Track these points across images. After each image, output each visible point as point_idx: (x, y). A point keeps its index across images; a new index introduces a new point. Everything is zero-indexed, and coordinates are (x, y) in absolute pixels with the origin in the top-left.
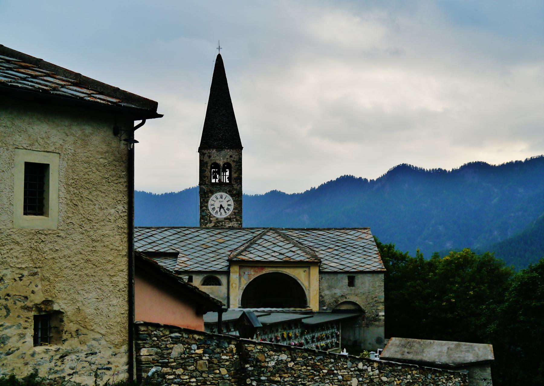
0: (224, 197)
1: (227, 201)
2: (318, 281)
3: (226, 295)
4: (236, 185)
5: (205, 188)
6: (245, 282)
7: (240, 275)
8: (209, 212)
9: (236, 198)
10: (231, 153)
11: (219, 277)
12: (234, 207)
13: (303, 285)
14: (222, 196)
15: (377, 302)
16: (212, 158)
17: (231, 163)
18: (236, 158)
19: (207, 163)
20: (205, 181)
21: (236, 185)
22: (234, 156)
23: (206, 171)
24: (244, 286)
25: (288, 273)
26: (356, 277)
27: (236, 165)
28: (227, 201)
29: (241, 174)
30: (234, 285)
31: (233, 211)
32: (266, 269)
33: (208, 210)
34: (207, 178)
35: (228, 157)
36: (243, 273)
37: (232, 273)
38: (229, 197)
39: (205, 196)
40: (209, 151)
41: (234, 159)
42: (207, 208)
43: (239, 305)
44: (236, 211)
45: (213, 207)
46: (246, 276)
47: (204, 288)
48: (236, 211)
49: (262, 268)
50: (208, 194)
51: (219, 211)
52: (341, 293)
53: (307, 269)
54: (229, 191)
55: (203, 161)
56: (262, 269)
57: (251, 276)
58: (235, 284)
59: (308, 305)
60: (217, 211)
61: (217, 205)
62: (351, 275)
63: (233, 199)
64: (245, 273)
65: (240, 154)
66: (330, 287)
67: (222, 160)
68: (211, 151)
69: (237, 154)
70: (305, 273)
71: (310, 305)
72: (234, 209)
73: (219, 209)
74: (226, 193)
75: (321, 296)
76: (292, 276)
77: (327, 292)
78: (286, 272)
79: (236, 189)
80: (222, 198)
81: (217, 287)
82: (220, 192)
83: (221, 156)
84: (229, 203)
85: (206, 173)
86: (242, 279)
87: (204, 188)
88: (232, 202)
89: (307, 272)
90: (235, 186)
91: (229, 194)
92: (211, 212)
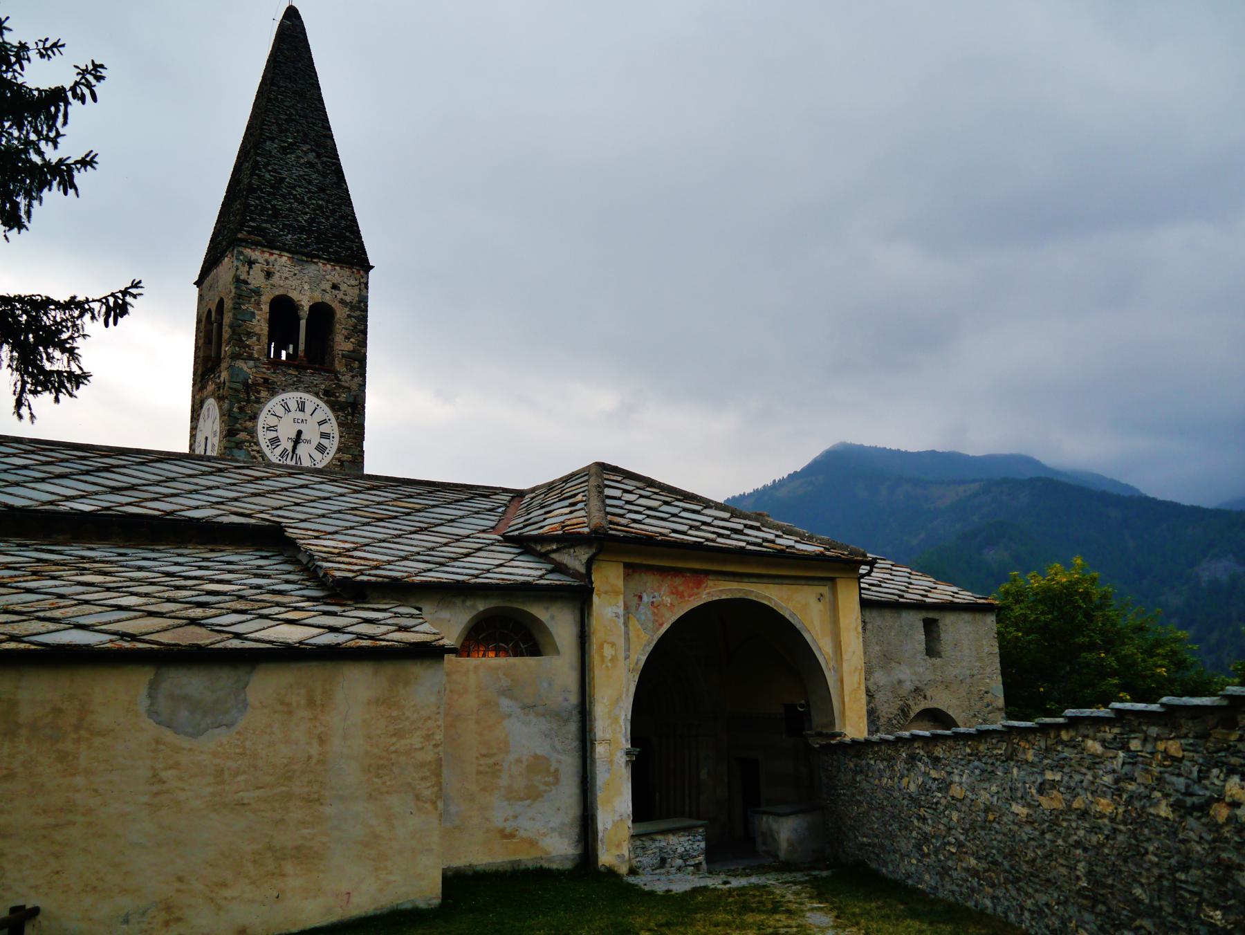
0: (309, 409)
1: (320, 423)
2: (861, 639)
3: (574, 699)
4: (348, 377)
5: (248, 370)
6: (645, 637)
7: (626, 607)
8: (258, 452)
9: (347, 415)
10: (336, 279)
11: (540, 612)
12: (340, 442)
13: (820, 649)
14: (303, 403)
15: (990, 707)
16: (275, 279)
17: (335, 305)
18: (352, 295)
19: (257, 292)
20: (249, 346)
21: (348, 377)
22: (343, 287)
23: (253, 315)
24: (640, 656)
25: (776, 603)
26: (940, 624)
27: (349, 316)
28: (320, 423)
29: (363, 343)
30: (608, 651)
31: (337, 456)
32: (710, 583)
33: (257, 444)
34: (258, 340)
35: (328, 286)
36: (636, 599)
37: (599, 595)
38: (325, 412)
39: (249, 396)
40: (267, 255)
41: (344, 297)
42: (252, 437)
43: (627, 741)
44: (346, 457)
45: (273, 435)
46: (645, 612)
47: (476, 667)
48: (346, 457)
49: (700, 576)
50: (259, 392)
51: (290, 449)
52: (914, 678)
53: (825, 590)
54: (326, 393)
55: (246, 282)
56: (699, 584)
57: (663, 610)
58: (613, 644)
59: (837, 730)
60: (285, 450)
61: (286, 432)
62: (931, 615)
63: (337, 418)
64: (640, 598)
65: (363, 286)
66: (888, 659)
67: (308, 293)
68: (272, 258)
69: (354, 283)
70: (820, 606)
71: (844, 725)
72: (339, 450)
73: (292, 444)
74: (317, 395)
75: (868, 691)
76: (787, 616)
77: (880, 677)
78: (769, 599)
79: (348, 388)
80: (302, 410)
81: (531, 661)
82: (297, 389)
83: (306, 279)
84: (325, 428)
85: (255, 322)
86: (634, 624)
87: (245, 369)
88: (333, 428)
89: (827, 600)
90: (346, 379)
91: (326, 402)
92: (267, 451)
